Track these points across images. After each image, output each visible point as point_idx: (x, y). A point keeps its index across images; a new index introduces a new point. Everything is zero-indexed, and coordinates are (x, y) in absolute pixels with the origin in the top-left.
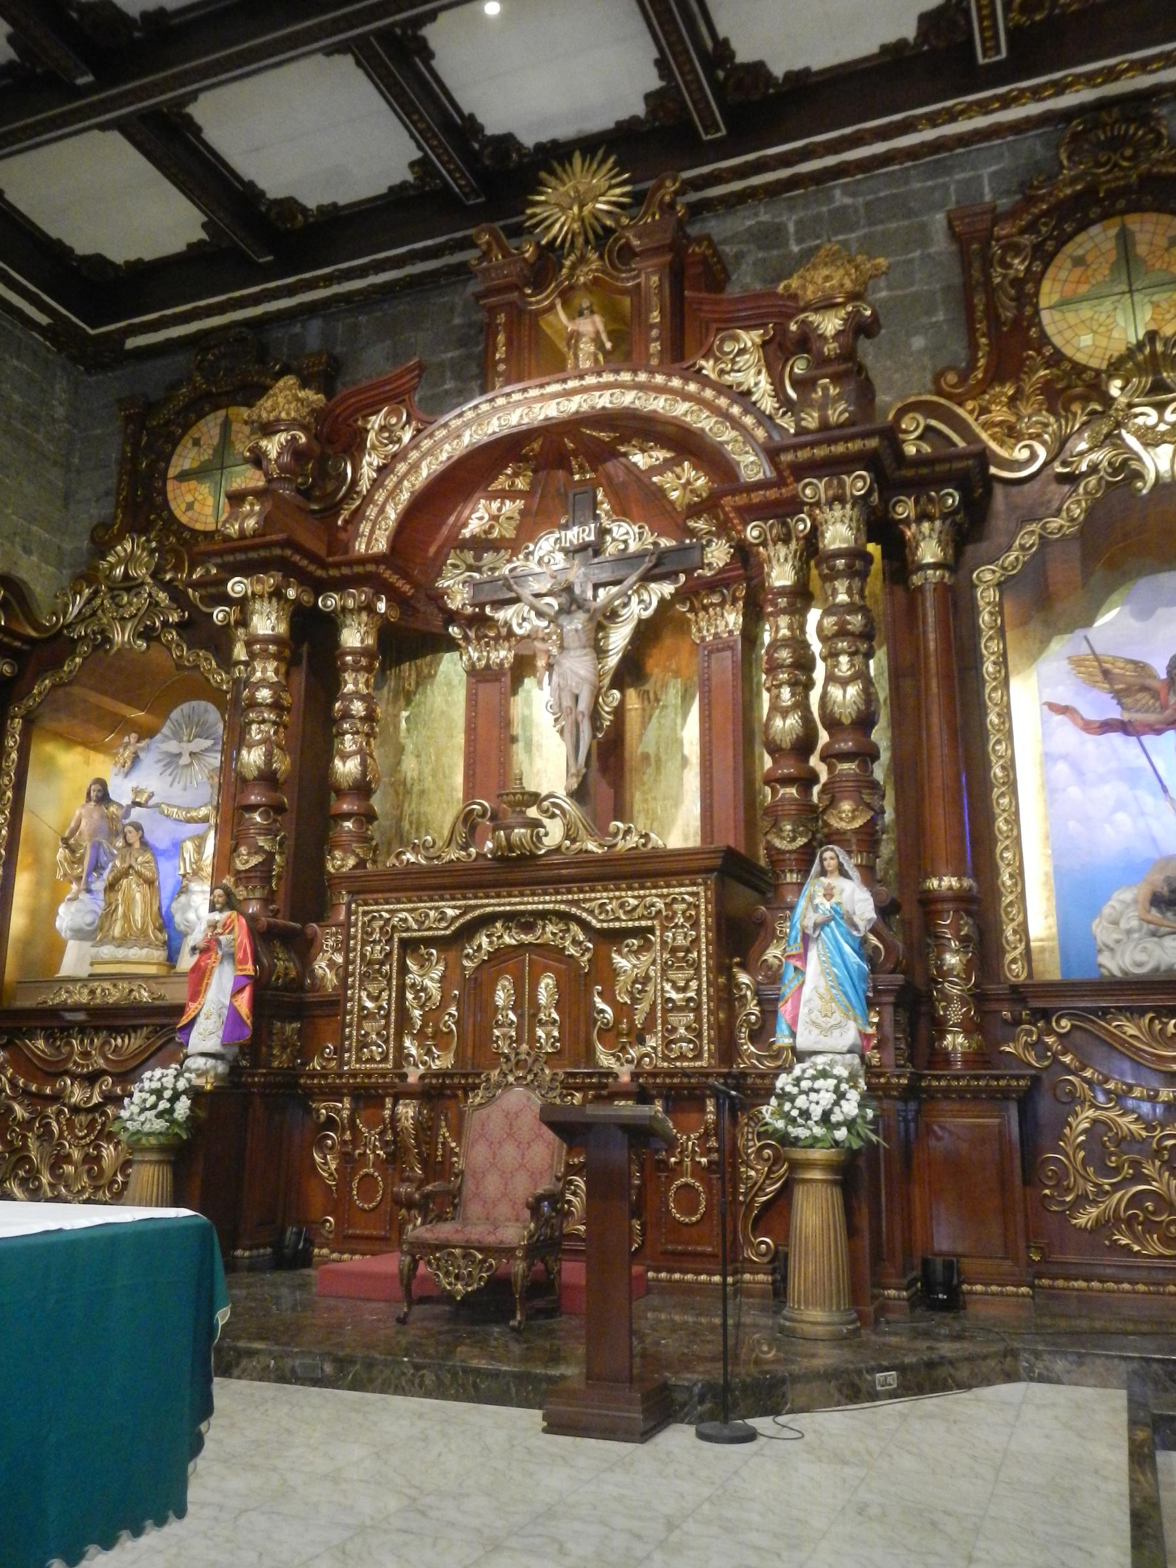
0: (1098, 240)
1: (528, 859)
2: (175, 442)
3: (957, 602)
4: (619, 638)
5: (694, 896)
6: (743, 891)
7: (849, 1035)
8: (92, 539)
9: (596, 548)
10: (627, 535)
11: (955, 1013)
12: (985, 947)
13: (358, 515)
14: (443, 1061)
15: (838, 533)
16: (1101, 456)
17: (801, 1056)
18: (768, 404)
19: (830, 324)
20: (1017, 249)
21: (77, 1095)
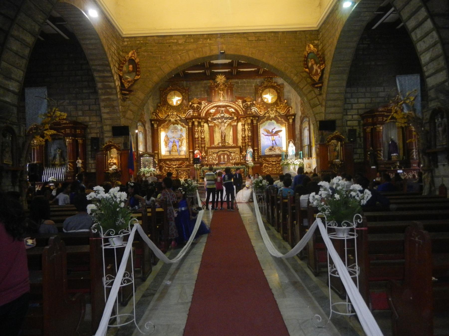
0: (267, 90)
1: (225, 146)
2: (168, 94)
3: (257, 126)
4: (226, 125)
5: (238, 149)
6: (242, 150)
7: (251, 159)
8: (158, 104)
9: (224, 116)
10: (227, 115)
11: (256, 158)
12: (258, 153)
13: (202, 112)
14: (217, 162)
15: (249, 121)
16: (268, 115)
17: (248, 161)
18: (242, 107)
19: (249, 103)
20: (260, 90)
21: (174, 167)
